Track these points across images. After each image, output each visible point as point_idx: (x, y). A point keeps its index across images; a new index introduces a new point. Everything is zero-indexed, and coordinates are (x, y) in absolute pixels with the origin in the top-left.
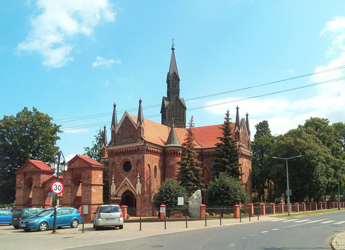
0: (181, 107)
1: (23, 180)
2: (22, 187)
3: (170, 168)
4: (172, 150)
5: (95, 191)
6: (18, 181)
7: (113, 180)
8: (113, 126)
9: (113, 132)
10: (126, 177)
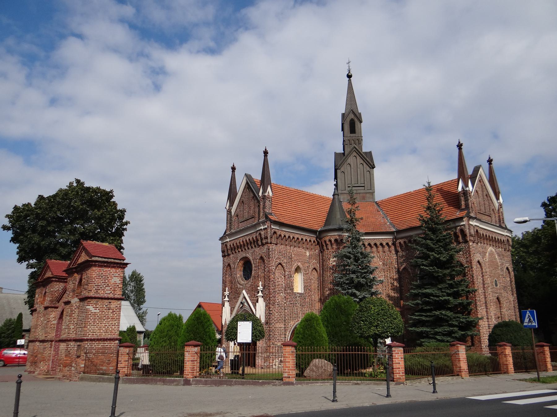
0: (365, 164)
5: (98, 311)
7: (227, 296)
10: (244, 292)
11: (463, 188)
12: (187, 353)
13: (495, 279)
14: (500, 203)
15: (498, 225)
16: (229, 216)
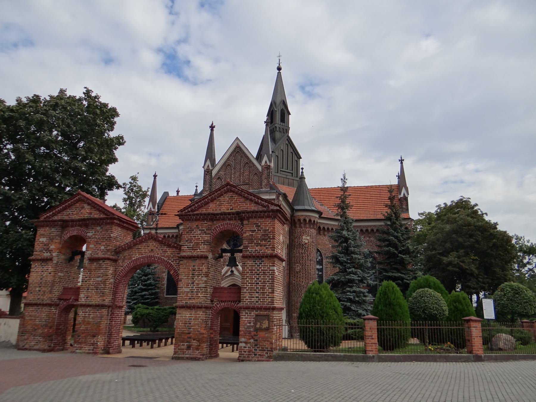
1: (57, 241)
2: (51, 259)
3: (302, 249)
4: (306, 216)
6: (43, 242)
8: (208, 162)
9: (208, 172)
11: (404, 194)
12: (474, 329)
16: (208, 177)
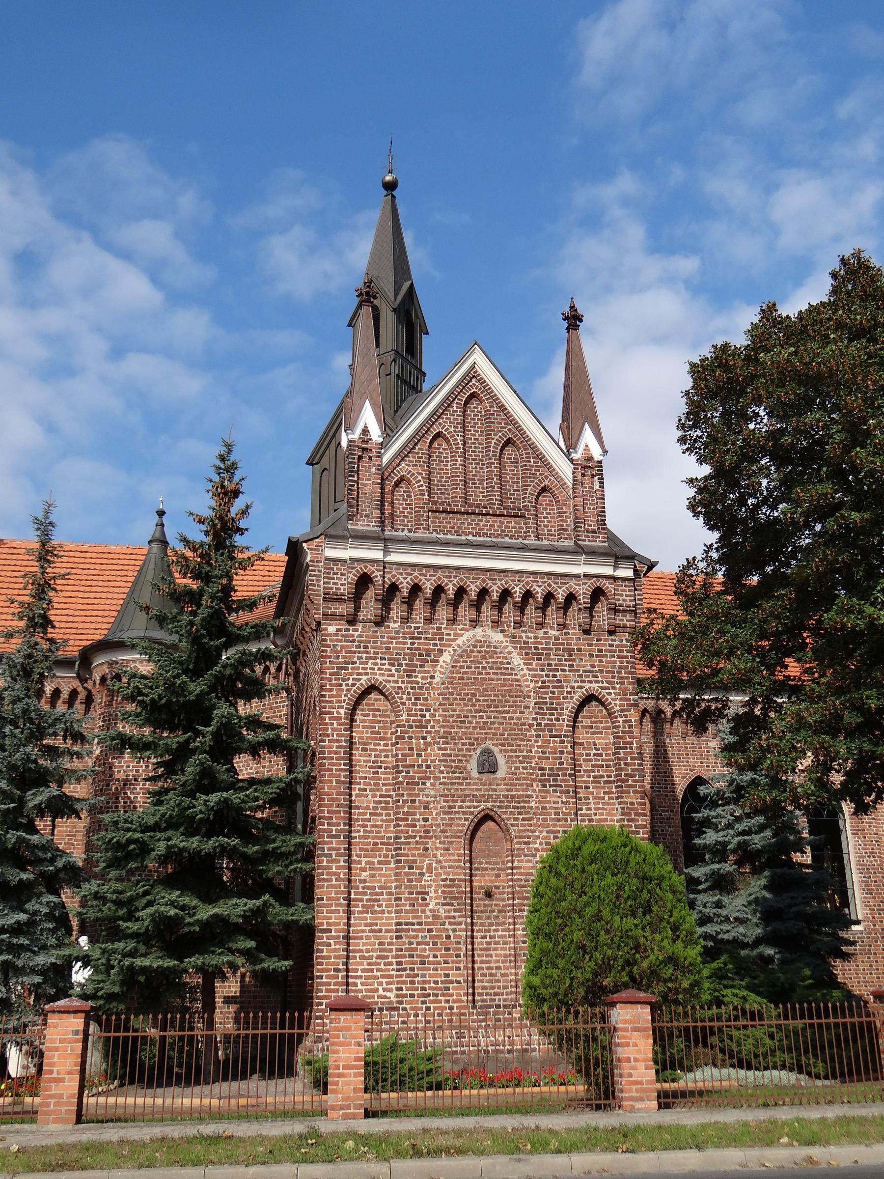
13: (489, 744)
14: (590, 458)
15: (569, 543)
